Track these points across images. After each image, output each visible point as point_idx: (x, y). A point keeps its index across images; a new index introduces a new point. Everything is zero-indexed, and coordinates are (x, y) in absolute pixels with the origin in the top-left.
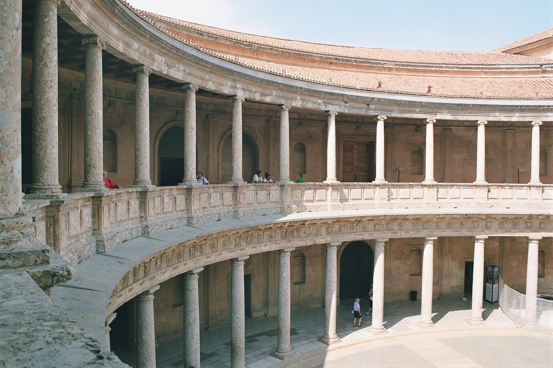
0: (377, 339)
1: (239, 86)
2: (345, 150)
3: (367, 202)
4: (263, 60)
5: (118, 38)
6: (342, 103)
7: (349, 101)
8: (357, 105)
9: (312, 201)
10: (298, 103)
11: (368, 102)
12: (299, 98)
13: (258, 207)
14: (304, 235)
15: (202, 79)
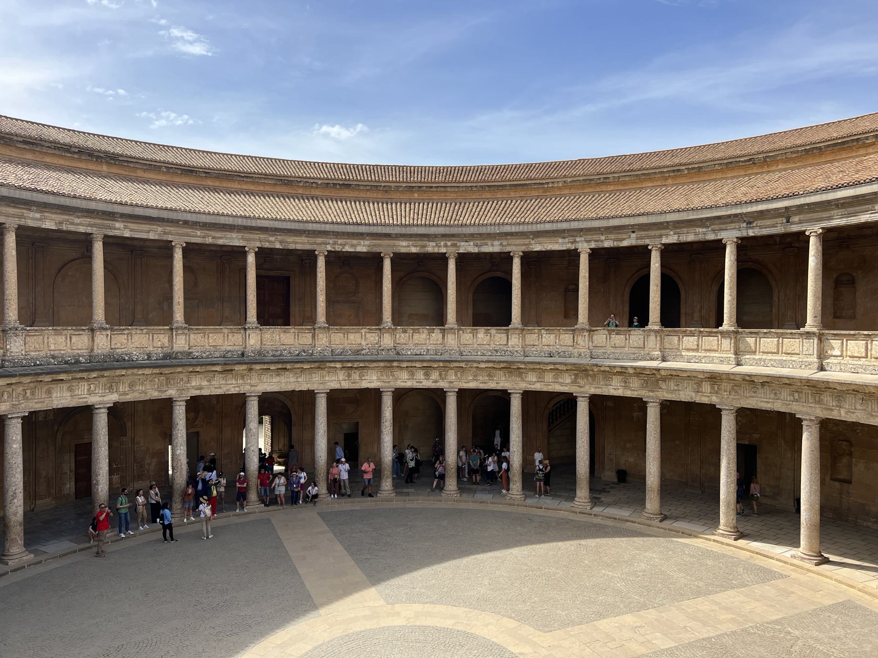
0: (792, 565)
1: (578, 239)
2: (838, 283)
3: (788, 358)
4: (780, 171)
5: (409, 246)
6: (745, 225)
7: (756, 220)
8: (768, 222)
9: (697, 350)
10: (671, 238)
11: (787, 214)
12: (672, 233)
13: (610, 350)
14: (676, 388)
15: (524, 245)
